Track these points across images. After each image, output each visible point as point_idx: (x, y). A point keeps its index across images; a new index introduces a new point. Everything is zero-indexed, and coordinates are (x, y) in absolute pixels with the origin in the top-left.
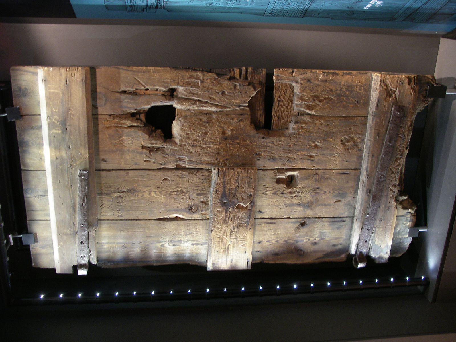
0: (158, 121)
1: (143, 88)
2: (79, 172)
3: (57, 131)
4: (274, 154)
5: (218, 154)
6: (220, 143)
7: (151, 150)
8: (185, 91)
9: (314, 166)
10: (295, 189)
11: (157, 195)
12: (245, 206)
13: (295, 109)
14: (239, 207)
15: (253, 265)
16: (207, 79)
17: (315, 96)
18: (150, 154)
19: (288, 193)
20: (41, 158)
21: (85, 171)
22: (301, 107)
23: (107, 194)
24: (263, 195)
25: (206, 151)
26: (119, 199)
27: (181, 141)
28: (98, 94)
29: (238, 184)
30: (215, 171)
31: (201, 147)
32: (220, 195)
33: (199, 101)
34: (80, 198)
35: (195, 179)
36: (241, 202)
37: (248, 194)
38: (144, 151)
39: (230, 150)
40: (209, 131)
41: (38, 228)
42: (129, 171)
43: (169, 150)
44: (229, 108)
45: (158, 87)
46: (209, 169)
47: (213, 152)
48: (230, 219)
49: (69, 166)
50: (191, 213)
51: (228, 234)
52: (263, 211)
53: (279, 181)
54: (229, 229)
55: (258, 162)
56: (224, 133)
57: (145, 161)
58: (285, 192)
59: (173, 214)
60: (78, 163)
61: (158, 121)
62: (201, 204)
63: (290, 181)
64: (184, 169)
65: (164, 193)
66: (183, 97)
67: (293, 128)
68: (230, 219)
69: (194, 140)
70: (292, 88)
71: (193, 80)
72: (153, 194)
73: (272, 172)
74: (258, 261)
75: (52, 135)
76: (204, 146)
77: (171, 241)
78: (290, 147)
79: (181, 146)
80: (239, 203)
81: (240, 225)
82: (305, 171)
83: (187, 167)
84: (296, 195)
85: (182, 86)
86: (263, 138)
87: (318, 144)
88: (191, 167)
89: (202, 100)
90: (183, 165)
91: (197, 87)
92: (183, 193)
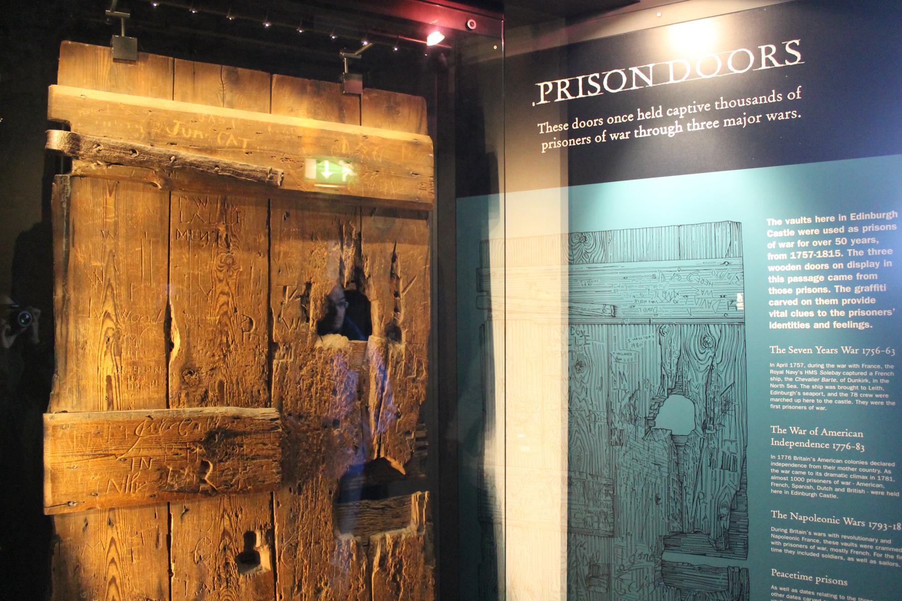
0: (349, 312)
1: (401, 289)
2: (280, 171)
3: (344, 147)
4: (302, 517)
5: (300, 417)
6: (319, 418)
7: (305, 298)
8: (399, 353)
9: (281, 597)
10: (234, 572)
11: (220, 307)
12: (206, 478)
13: (377, 537)
14: (205, 465)
15: (50, 518)
16: (417, 388)
17: (401, 566)
18: (297, 297)
19: (226, 559)
20: (292, 110)
21: (281, 182)
22: (382, 546)
23: (224, 212)
24: (221, 511)
25: (305, 394)
26: (214, 235)
27: (321, 350)
28: (392, 219)
29: (253, 459)
30: (272, 412)
31: (311, 386)
32: (229, 427)
33: (385, 378)
34: (229, 166)
35: (252, 378)
36: (214, 469)
37: (231, 480)
38: (304, 287)
39: (308, 437)
40: (338, 397)
41: (145, 72)
42: (266, 258)
43: (304, 330)
44: (376, 428)
45: (403, 311)
46: (270, 401)
47: (302, 408)
48: (179, 452)
49: (286, 156)
50: (182, 371)
51: (144, 452)
52: (186, 517)
53: (250, 538)
54: (154, 452)
55: (286, 490)
56: (336, 423)
57: (285, 288)
58: (228, 552)
59: (181, 338)
60: (292, 172)
61: (349, 312)
62: (201, 391)
63: (249, 559)
64: (270, 358)
65: (225, 319)
66: (391, 352)
67: (348, 542)
68: (179, 452)
69: (322, 373)
70: (404, 524)
71: (415, 366)
72: (223, 299)
73: (268, 520)
74: (58, 529)
75: (338, 138)
76: (313, 390)
77: (118, 332)
78: (316, 543)
79: (313, 350)
80: (211, 465)
81: (162, 472)
82: (273, 581)
83: (275, 362)
84: (223, 575)
85: (406, 349)
86: (330, 493)
87: (323, 594)
88: (274, 370)
89: (387, 382)
90: (277, 355)
91: (406, 373)
92: (225, 356)
